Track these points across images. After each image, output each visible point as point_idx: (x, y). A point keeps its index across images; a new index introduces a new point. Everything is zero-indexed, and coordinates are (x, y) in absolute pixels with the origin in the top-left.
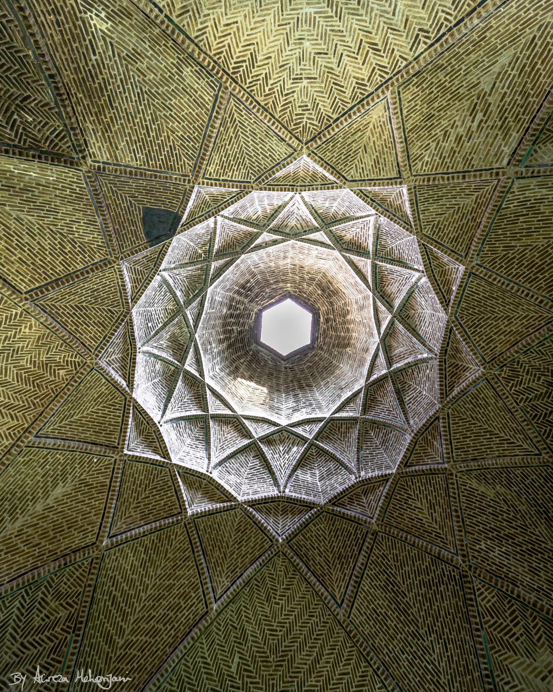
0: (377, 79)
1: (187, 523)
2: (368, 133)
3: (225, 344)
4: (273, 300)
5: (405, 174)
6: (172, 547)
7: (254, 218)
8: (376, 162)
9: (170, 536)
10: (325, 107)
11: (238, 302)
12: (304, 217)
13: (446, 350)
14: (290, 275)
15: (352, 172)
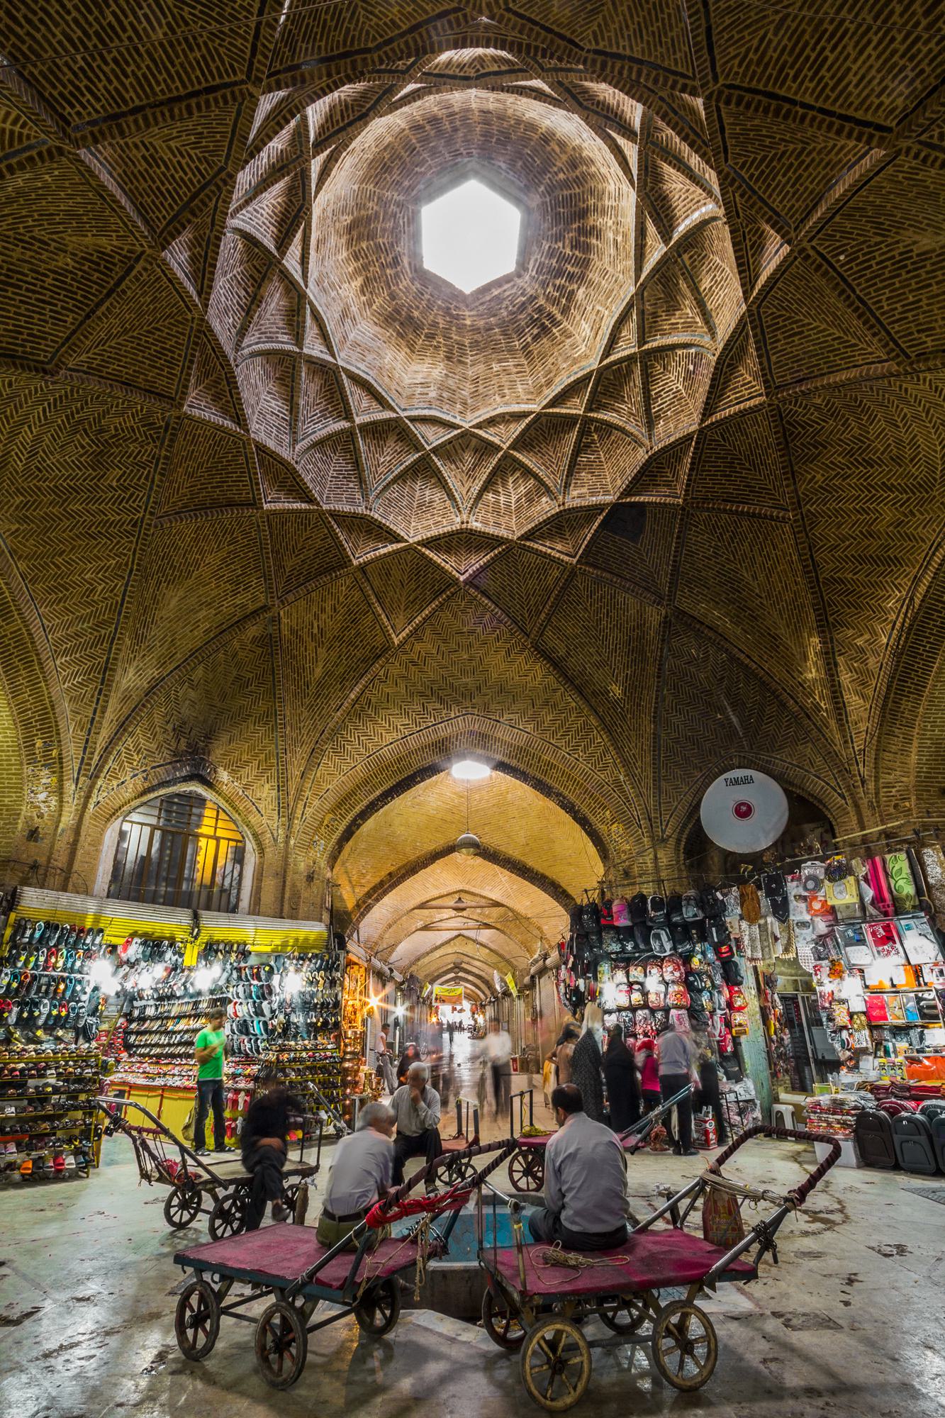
0: (407, 647)
3: (592, 223)
4: (496, 293)
5: (359, 575)
7: (517, 474)
8: (388, 574)
11: (555, 302)
13: (229, 384)
14: (467, 342)
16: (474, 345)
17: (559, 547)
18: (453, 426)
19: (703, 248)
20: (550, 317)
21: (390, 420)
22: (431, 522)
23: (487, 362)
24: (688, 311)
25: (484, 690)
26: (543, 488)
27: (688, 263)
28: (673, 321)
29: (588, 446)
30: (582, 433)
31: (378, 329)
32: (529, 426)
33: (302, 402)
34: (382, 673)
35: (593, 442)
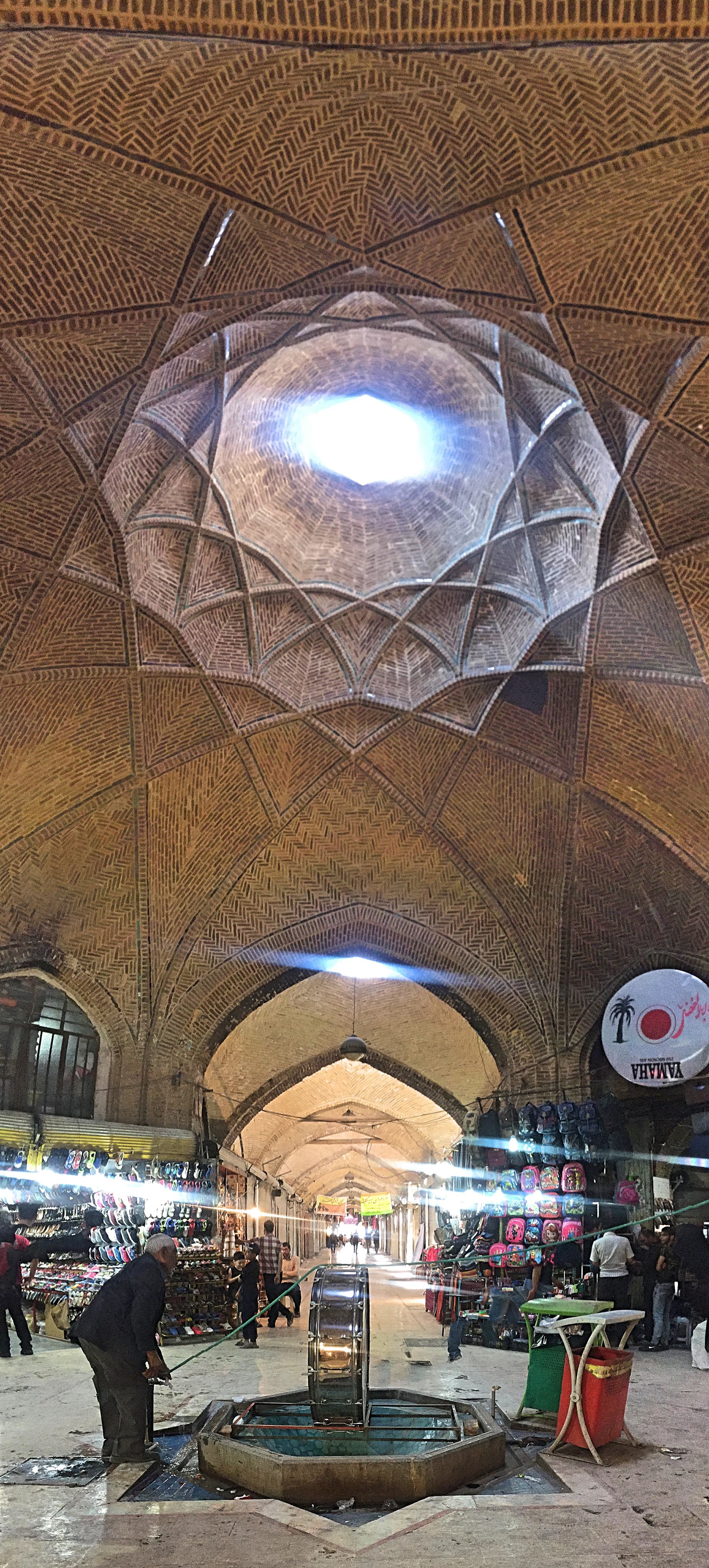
1: (549, 304)
2: (288, 774)
5: (242, 746)
6: (580, 270)
7: (413, 645)
8: (274, 746)
9: (583, 288)
10: (333, 793)
12: (348, 637)
14: (363, 525)
15: (298, 729)
16: (370, 526)
17: (458, 719)
18: (350, 599)
19: (570, 435)
20: (442, 503)
21: (285, 591)
22: (322, 692)
23: (383, 542)
24: (567, 489)
25: (376, 877)
26: (440, 659)
27: (559, 448)
28: (554, 498)
29: (484, 617)
30: (477, 605)
31: (278, 512)
32: (424, 598)
33: (195, 572)
34: (262, 855)
35: (489, 613)
